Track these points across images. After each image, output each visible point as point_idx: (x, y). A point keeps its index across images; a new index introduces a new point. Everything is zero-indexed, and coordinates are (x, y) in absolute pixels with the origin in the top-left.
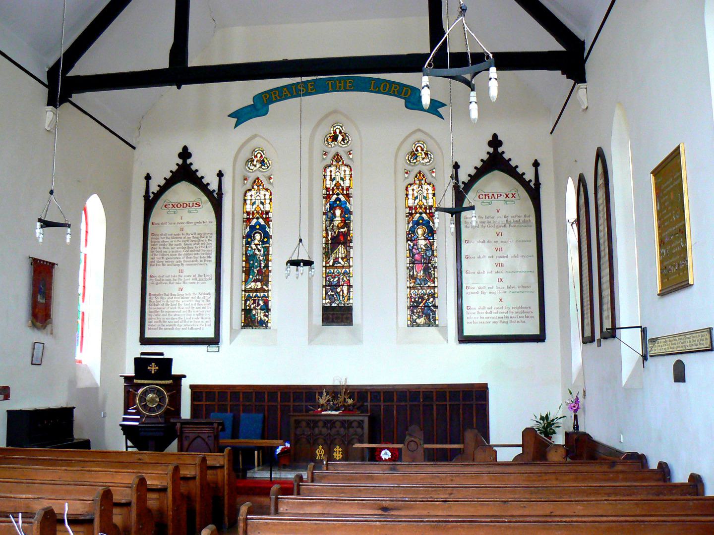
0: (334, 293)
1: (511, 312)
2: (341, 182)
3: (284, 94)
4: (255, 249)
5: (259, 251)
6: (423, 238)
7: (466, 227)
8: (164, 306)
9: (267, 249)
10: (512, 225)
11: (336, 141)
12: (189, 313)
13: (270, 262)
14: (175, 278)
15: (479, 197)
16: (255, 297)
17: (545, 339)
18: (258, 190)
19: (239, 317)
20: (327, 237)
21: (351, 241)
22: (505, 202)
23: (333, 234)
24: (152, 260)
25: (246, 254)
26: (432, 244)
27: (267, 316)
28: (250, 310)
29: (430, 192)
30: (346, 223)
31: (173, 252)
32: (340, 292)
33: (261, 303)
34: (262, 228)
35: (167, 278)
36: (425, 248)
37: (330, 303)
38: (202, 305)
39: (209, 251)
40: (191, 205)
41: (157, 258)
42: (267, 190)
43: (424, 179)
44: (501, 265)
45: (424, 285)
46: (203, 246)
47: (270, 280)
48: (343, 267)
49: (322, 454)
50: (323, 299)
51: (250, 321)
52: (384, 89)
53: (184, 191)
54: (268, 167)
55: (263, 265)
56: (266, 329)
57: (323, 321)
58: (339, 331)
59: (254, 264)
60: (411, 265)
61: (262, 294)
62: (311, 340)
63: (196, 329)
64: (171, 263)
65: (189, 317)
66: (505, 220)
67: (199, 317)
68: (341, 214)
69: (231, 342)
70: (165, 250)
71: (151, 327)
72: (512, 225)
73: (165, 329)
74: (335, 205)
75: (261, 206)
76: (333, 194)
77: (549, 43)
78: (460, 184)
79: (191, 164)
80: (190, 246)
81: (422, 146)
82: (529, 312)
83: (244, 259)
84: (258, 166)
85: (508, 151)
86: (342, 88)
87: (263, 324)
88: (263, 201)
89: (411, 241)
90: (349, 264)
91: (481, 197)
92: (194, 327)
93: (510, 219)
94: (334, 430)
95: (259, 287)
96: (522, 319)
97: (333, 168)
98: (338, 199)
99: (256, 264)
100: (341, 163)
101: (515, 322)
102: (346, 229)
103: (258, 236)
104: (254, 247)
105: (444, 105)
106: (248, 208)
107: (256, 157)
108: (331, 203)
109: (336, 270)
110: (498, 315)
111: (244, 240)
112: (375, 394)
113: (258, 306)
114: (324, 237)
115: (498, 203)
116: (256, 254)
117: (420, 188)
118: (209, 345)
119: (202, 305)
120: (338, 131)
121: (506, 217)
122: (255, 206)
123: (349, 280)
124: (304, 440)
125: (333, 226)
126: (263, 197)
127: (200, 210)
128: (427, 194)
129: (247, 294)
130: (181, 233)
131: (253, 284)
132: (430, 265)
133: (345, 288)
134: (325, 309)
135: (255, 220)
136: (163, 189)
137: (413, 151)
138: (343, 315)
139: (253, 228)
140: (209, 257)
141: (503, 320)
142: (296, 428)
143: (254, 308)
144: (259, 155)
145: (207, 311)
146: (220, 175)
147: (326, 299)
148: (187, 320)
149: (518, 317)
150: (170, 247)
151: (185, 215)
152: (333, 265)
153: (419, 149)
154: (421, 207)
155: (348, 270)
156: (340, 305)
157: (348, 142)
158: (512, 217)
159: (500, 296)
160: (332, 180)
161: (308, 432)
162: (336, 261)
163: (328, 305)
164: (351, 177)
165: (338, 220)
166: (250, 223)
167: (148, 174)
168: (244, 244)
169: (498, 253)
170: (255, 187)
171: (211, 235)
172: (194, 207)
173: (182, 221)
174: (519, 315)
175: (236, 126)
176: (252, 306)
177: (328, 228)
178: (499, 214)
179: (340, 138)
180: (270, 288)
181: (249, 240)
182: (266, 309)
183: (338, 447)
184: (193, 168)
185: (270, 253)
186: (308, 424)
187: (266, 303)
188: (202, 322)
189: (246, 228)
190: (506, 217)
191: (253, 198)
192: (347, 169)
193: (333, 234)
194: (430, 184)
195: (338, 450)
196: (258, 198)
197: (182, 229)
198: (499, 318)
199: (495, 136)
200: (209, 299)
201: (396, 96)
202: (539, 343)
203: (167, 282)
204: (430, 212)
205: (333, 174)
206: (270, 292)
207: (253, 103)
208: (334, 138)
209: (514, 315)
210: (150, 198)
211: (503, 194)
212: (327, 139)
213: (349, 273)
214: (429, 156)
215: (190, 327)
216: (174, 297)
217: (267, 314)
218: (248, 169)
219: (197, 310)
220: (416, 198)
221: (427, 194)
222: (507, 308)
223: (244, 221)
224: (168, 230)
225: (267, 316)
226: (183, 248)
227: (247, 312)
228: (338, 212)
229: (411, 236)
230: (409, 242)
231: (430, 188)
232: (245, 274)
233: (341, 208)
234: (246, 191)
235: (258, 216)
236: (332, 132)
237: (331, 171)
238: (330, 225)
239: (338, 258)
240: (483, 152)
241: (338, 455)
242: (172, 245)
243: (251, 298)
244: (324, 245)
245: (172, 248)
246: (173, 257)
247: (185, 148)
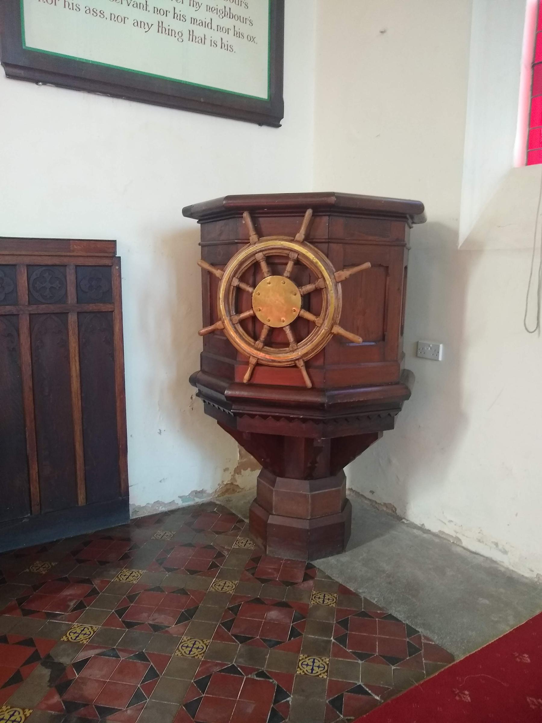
17: (281, 116)
82: (244, 20)
101: (203, 41)
141: (170, 22)
149: (214, 27)
174: (217, 21)
202: (265, 129)
209: (203, 15)
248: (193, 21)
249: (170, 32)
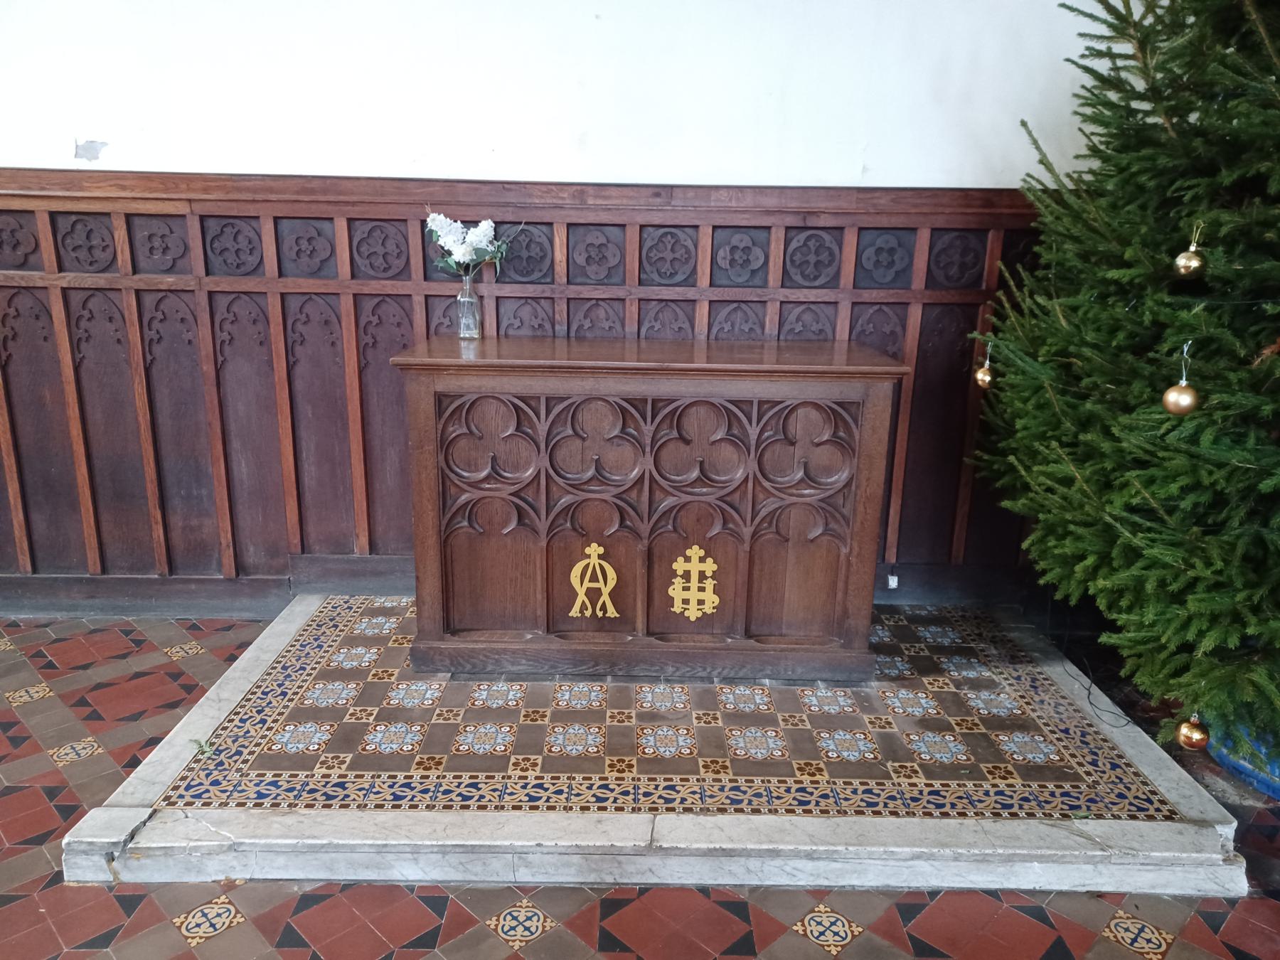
49: (606, 591)
142: (446, 446)
183: (695, 552)
195: (695, 567)
241: (694, 595)
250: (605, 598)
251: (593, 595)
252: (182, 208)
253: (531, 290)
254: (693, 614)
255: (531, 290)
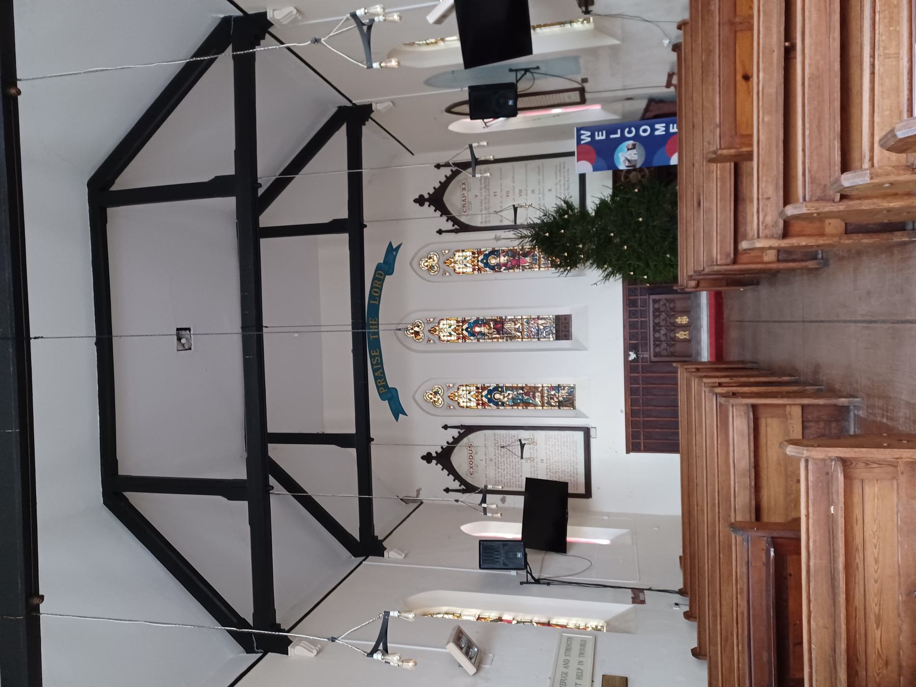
0: (544, 332)
1: (560, 181)
2: (453, 327)
3: (380, 375)
4: (508, 399)
5: (509, 394)
6: (498, 259)
7: (489, 222)
8: (557, 476)
9: (508, 388)
10: (487, 183)
11: (419, 332)
12: (563, 453)
13: (519, 385)
14: (533, 466)
15: (464, 212)
16: (548, 398)
18: (459, 396)
19: (565, 410)
20: (497, 338)
21: (501, 318)
22: (470, 190)
23: (495, 333)
24: (517, 487)
25: (512, 406)
26: (503, 251)
27: (564, 387)
28: (559, 402)
29: (460, 254)
30: (485, 323)
31: (510, 468)
32: (544, 326)
33: (553, 393)
34: (490, 392)
35: (533, 473)
36: (507, 257)
37: (552, 334)
38: (555, 442)
39: (509, 437)
40: (471, 452)
41: (516, 482)
42: (458, 389)
43: (450, 259)
44: (521, 191)
45: (537, 256)
46: (505, 441)
47: (534, 385)
48: (522, 324)
50: (550, 340)
51: (568, 402)
52: (376, 292)
53: (459, 459)
54: (439, 388)
55: (521, 392)
56: (575, 388)
57: (568, 339)
58: (576, 328)
59: (520, 399)
60: (521, 268)
61: (546, 392)
62: (585, 349)
63: (576, 447)
64: (520, 470)
65: (566, 454)
66: (483, 190)
67: (565, 444)
68: (479, 327)
69: (586, 417)
70: (509, 475)
71: (576, 488)
72: (487, 183)
73: (577, 475)
74: (472, 332)
75: (472, 393)
76: (462, 334)
77: (340, 137)
78: (454, 228)
79: (436, 452)
80: (505, 453)
81: (424, 261)
82: (560, 166)
83: (516, 407)
84: (439, 397)
85: (427, 190)
86: (376, 327)
87: (572, 391)
88: (468, 392)
89: (500, 268)
90: (520, 319)
91: (465, 210)
92: (575, 449)
93: (483, 185)
94: (662, 323)
95: (539, 394)
96: (566, 171)
97: (441, 335)
98: (466, 330)
99: (520, 397)
100: (437, 328)
101: (568, 178)
102: (491, 323)
103: (497, 396)
104: (506, 399)
105: (390, 244)
106: (473, 404)
107: (431, 398)
108: (470, 335)
109: (525, 330)
110: (563, 192)
111: (500, 407)
112: (630, 292)
113: (556, 395)
114: (498, 341)
115: (470, 196)
116: (512, 398)
117: (458, 262)
118: (590, 436)
119: (555, 442)
120: (411, 331)
121: (481, 190)
122: (472, 399)
123: (533, 319)
124: (671, 349)
125: (489, 333)
126: (465, 392)
127: (475, 444)
128: (462, 256)
129: (546, 405)
130: (494, 460)
131: (537, 400)
132: (521, 252)
133: (540, 322)
134: (558, 338)
135: (484, 398)
136: (457, 477)
137: (428, 269)
138: (562, 323)
139: (490, 400)
140: (514, 436)
141: (566, 187)
142: (661, 356)
143: (557, 398)
144: (430, 396)
145: (561, 437)
146: (446, 427)
147: (549, 338)
148: (569, 455)
150: (506, 470)
151: (479, 457)
152: (521, 333)
153: (426, 264)
154: (473, 261)
155: (525, 320)
156: (554, 326)
157: (420, 323)
158: (481, 184)
159: (546, 191)
160: (451, 335)
161: (664, 345)
162: (517, 330)
163: (554, 336)
164: (448, 319)
165: (483, 329)
166: (486, 403)
167: (444, 490)
168: (503, 408)
169: (511, 194)
170: (456, 398)
171: (496, 434)
172: (472, 450)
173: (484, 460)
174: (562, 174)
175: (405, 414)
176: (556, 400)
177: (490, 337)
178: (479, 194)
179: (416, 329)
180: (541, 385)
181: (500, 403)
182: (558, 388)
183: (677, 320)
184: (439, 450)
185: (511, 385)
186: (659, 345)
187: (552, 388)
188: (570, 442)
189: (490, 406)
190: (481, 190)
191: (465, 400)
192: (442, 322)
193: (495, 333)
194: (455, 255)
196: (465, 396)
197: (491, 460)
198: (564, 190)
199: (416, 201)
200: (551, 436)
201: (383, 282)
203: (536, 472)
204: (478, 254)
205: (446, 334)
206: (544, 385)
207: (387, 401)
208: (417, 333)
209: (562, 178)
210: (465, 488)
211: (462, 193)
212: (417, 339)
213: (527, 319)
214: (432, 256)
215: (575, 453)
216: (549, 467)
217: (562, 388)
218: (441, 405)
219: (560, 446)
220: (466, 265)
221: (462, 256)
222: (556, 185)
223: (485, 408)
224: (491, 473)
225: (564, 387)
226: (507, 459)
227: (561, 404)
228: (477, 329)
229: (495, 268)
230: (502, 270)
231: (457, 254)
232: (529, 406)
233: (474, 327)
234: (460, 406)
235: (480, 396)
236: (412, 335)
237: (444, 336)
238: (487, 335)
239: (515, 328)
240: (428, 210)
242: (504, 469)
243: (549, 401)
244: (504, 340)
245: (507, 469)
246: (514, 467)
247: (423, 458)
248: (564, 181)
249: (568, 187)
250: (685, 333)
251: (685, 335)
252: (630, 398)
253: (640, 346)
254: (688, 320)
255: (640, 346)
